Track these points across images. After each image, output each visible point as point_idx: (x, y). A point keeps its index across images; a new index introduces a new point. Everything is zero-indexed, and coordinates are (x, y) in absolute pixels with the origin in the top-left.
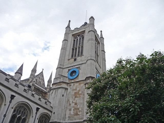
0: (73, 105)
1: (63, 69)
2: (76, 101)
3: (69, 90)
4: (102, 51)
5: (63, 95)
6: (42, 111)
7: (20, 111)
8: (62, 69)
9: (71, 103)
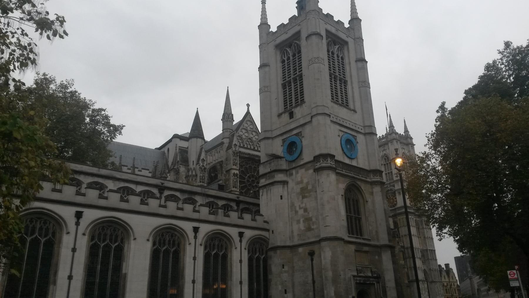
0: (301, 212)
1: (272, 138)
2: (305, 204)
3: (291, 184)
4: (356, 61)
5: (281, 196)
6: (249, 234)
7: (214, 245)
8: (270, 141)
9: (298, 209)
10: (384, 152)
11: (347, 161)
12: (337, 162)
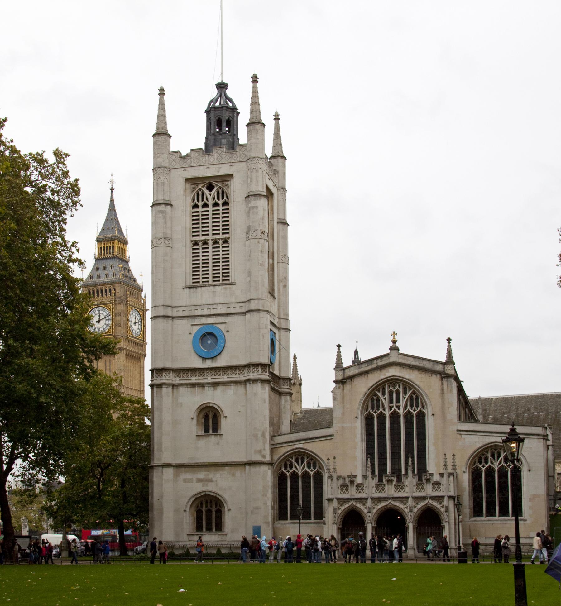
1: (173, 318)
4: (278, 223)
8: (170, 320)
12: (272, 374)
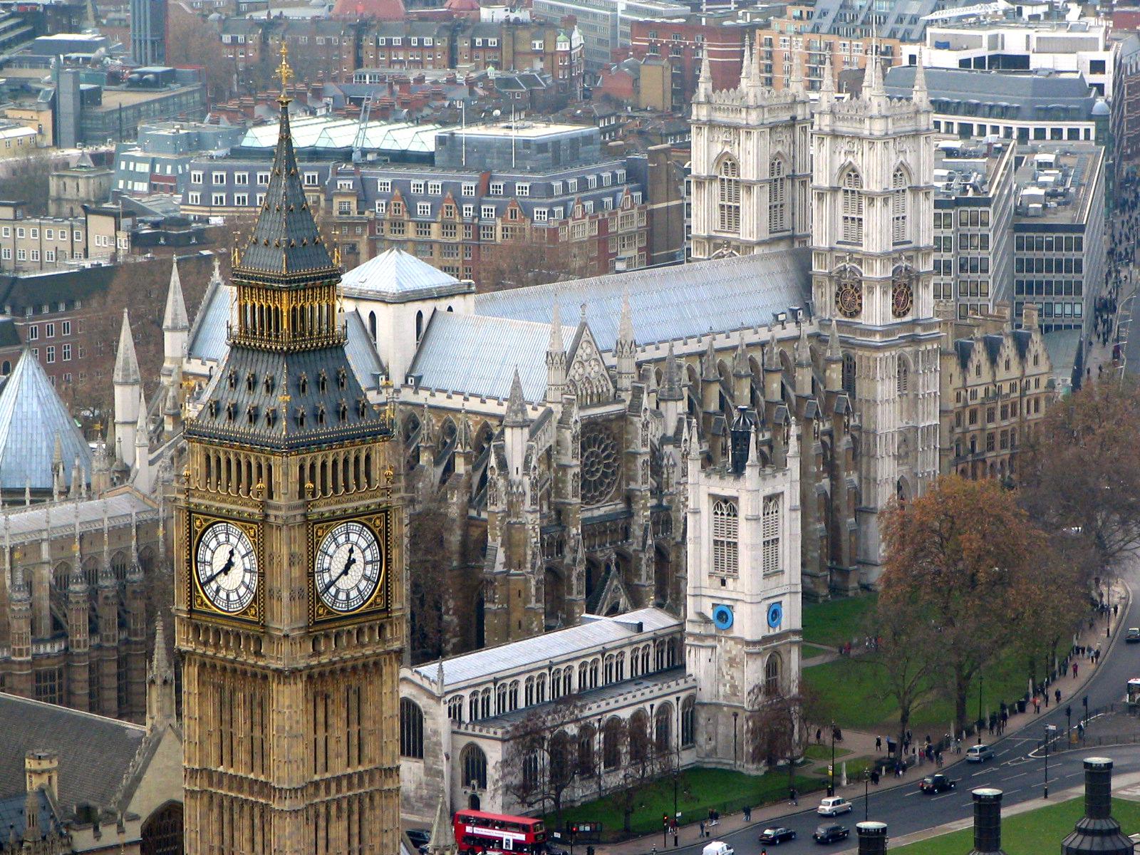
6: (683, 695)
10: (850, 158)
11: (772, 632)
